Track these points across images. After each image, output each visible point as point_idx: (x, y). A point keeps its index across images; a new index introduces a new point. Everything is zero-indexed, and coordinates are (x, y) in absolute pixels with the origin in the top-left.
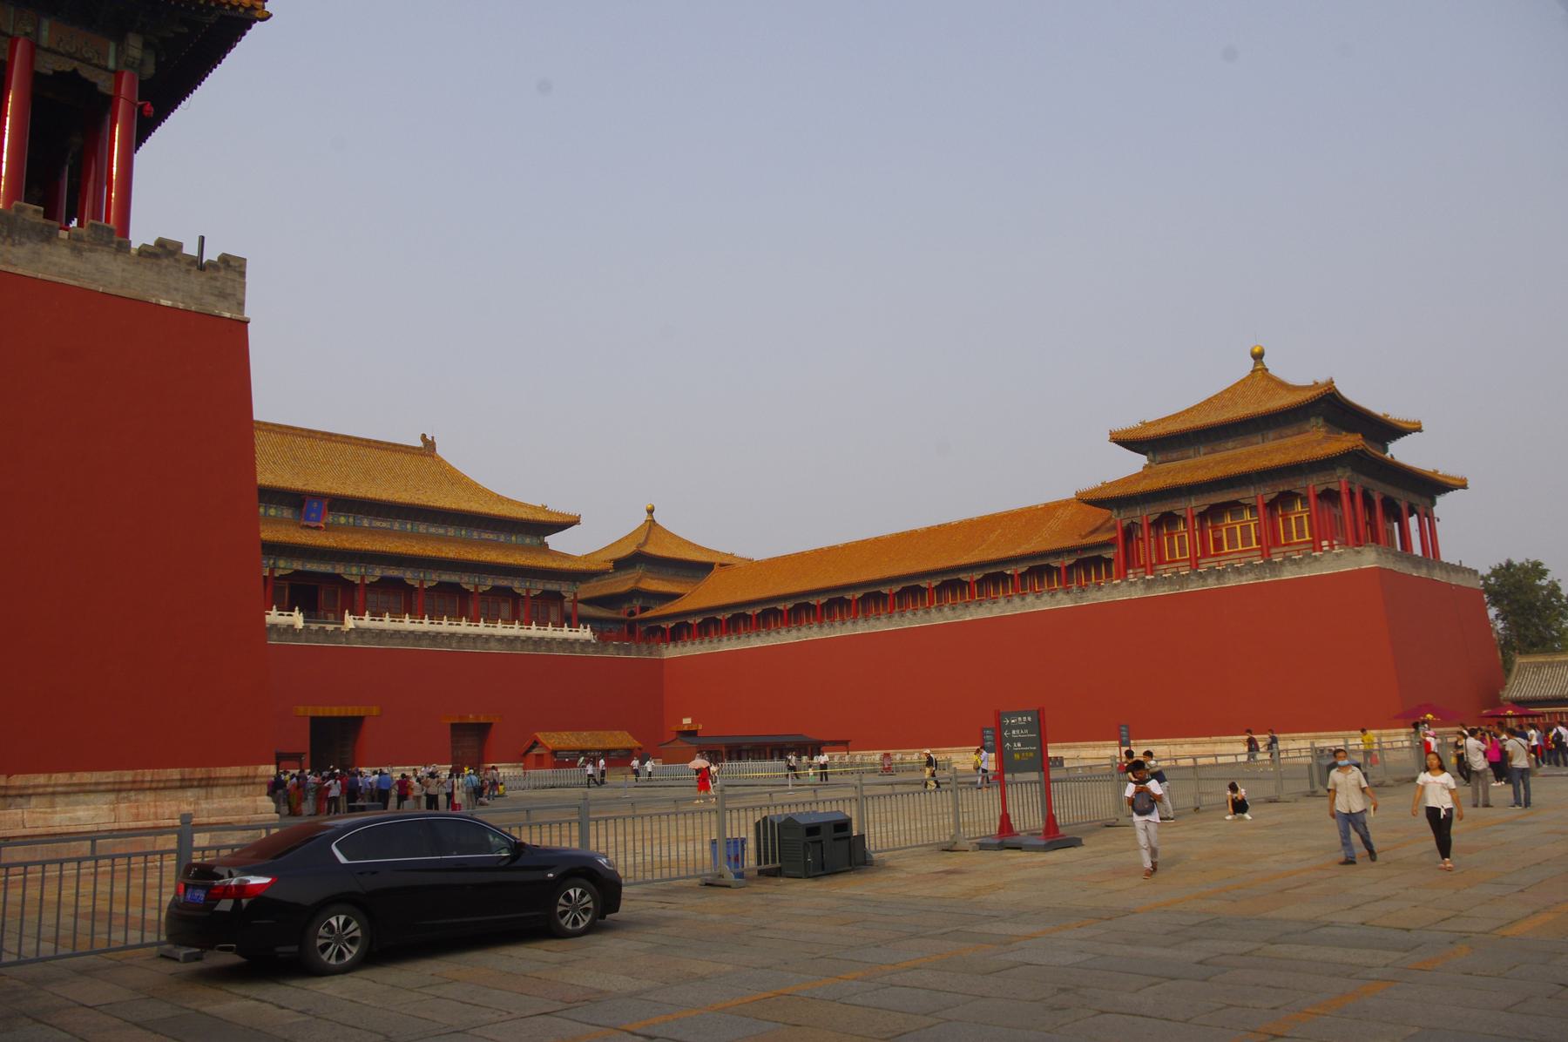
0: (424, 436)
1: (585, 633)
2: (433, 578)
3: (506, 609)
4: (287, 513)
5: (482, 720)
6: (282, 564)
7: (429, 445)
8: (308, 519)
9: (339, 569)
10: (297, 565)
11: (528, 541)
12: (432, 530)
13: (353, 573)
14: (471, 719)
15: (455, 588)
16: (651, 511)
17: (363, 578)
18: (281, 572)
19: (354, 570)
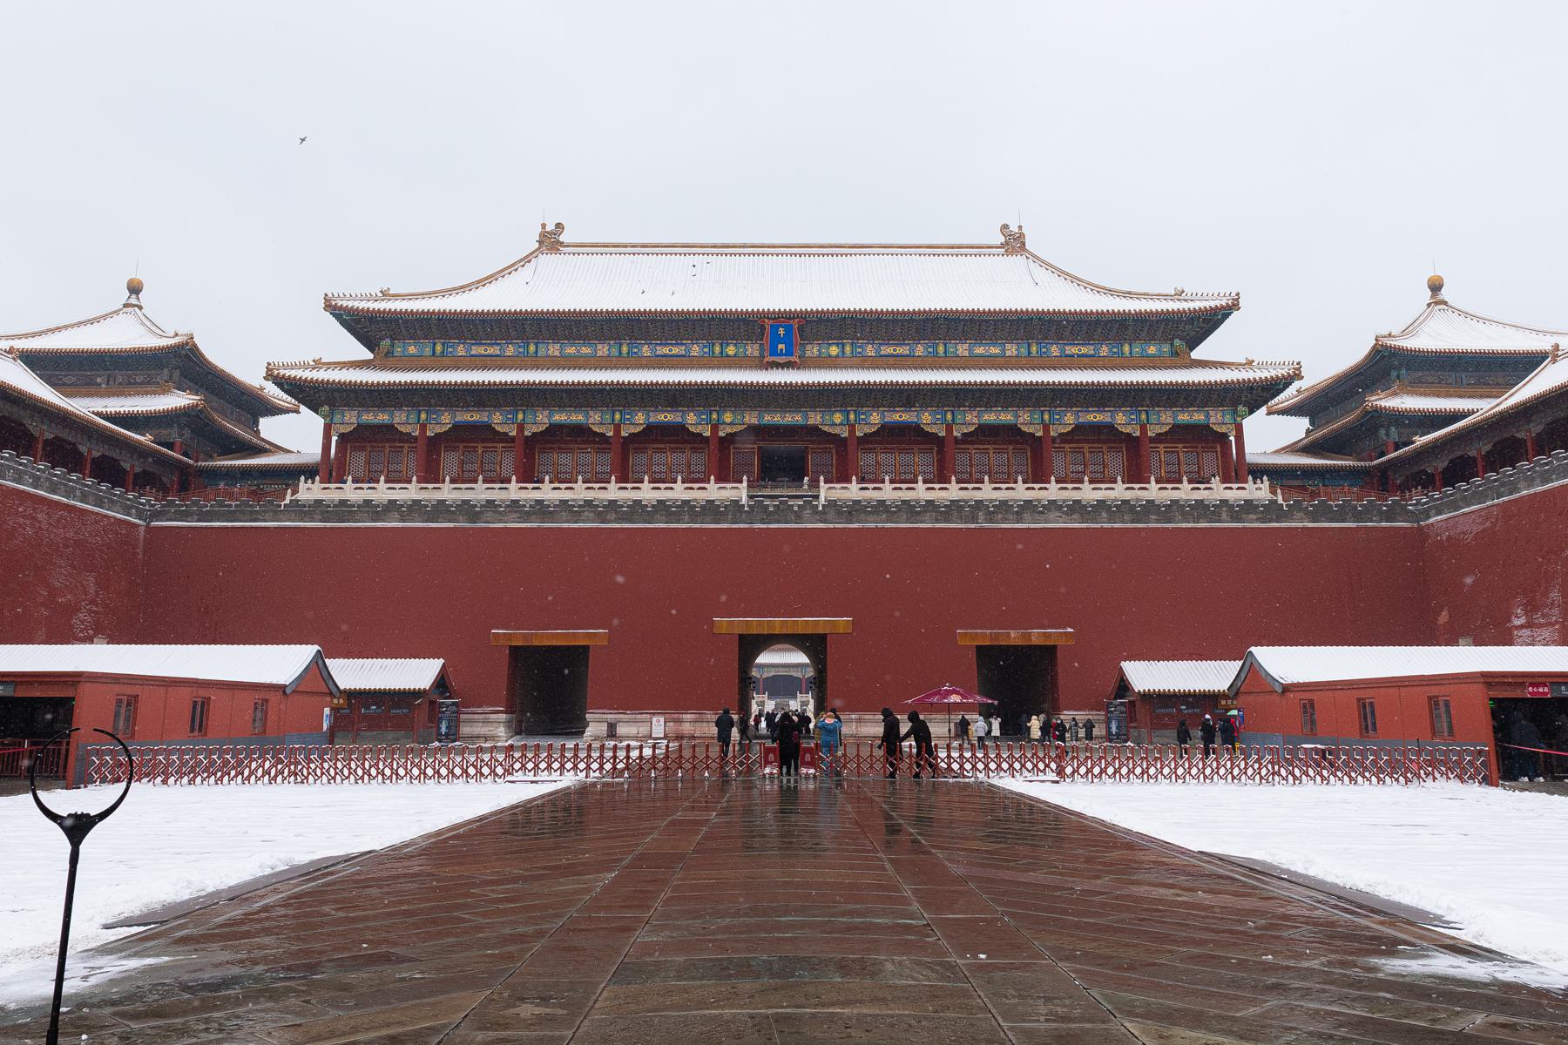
0: (1005, 227)
1: (1259, 491)
2: (969, 420)
3: (1116, 460)
4: (753, 350)
5: (1037, 636)
6: (728, 417)
7: (1014, 243)
8: (774, 352)
9: (815, 418)
10: (751, 418)
11: (1152, 350)
12: (979, 350)
13: (835, 422)
14: (1014, 637)
15: (1010, 434)
16: (1436, 287)
17: (852, 428)
18: (729, 430)
19: (838, 418)
